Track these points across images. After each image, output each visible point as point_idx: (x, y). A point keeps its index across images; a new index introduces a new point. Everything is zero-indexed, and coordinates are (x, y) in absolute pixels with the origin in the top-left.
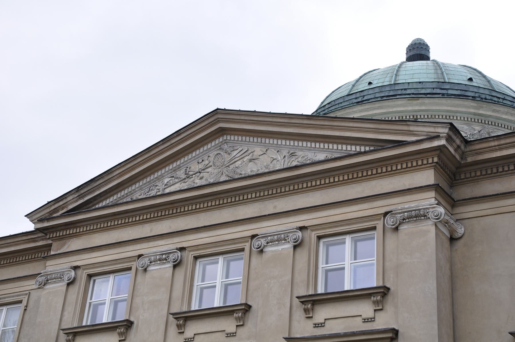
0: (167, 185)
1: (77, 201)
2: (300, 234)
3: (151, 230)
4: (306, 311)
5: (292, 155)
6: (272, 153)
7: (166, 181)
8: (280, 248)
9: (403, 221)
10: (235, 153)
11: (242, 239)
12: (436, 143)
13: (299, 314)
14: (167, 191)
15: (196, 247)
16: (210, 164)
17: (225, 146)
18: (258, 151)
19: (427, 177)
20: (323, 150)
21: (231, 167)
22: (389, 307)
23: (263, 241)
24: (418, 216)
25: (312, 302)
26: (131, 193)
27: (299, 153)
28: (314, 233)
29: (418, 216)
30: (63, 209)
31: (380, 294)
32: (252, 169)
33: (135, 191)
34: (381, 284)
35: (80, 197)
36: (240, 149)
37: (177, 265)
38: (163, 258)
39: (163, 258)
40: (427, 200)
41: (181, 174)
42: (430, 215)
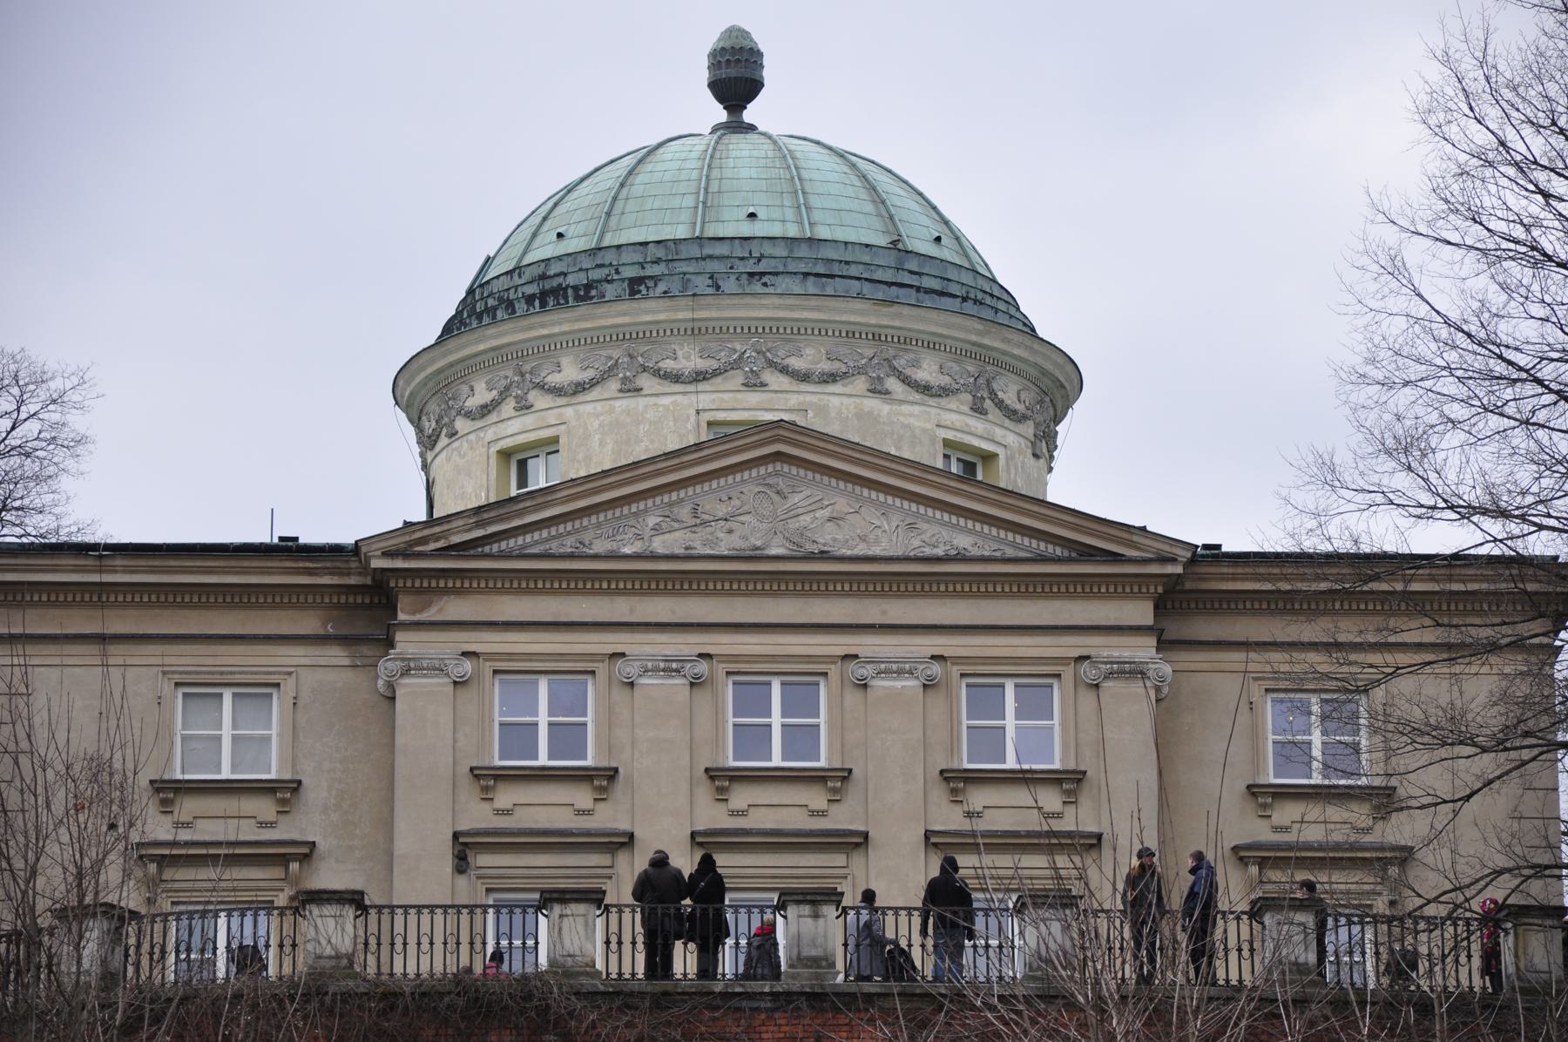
0: (657, 530)
1: (470, 530)
2: (936, 669)
3: (632, 611)
4: (954, 791)
5: (911, 527)
6: (871, 515)
7: (652, 521)
8: (899, 684)
9: (1109, 675)
10: (796, 498)
11: (830, 659)
12: (1170, 569)
13: (939, 793)
14: (659, 545)
15: (735, 658)
16: (746, 508)
17: (781, 483)
18: (842, 504)
19: (1141, 612)
20: (971, 532)
21: (793, 525)
22: (1085, 802)
23: (868, 671)
24: (1136, 672)
25: (957, 781)
26: (577, 531)
27: (925, 526)
28: (955, 668)
29: (1136, 672)
30: (437, 540)
31: (1070, 781)
32: (829, 537)
33: (586, 528)
34: (1072, 766)
35: (478, 525)
36: (808, 492)
37: (695, 684)
38: (670, 667)
39: (670, 667)
40: (1143, 650)
41: (684, 512)
42: (1151, 674)
